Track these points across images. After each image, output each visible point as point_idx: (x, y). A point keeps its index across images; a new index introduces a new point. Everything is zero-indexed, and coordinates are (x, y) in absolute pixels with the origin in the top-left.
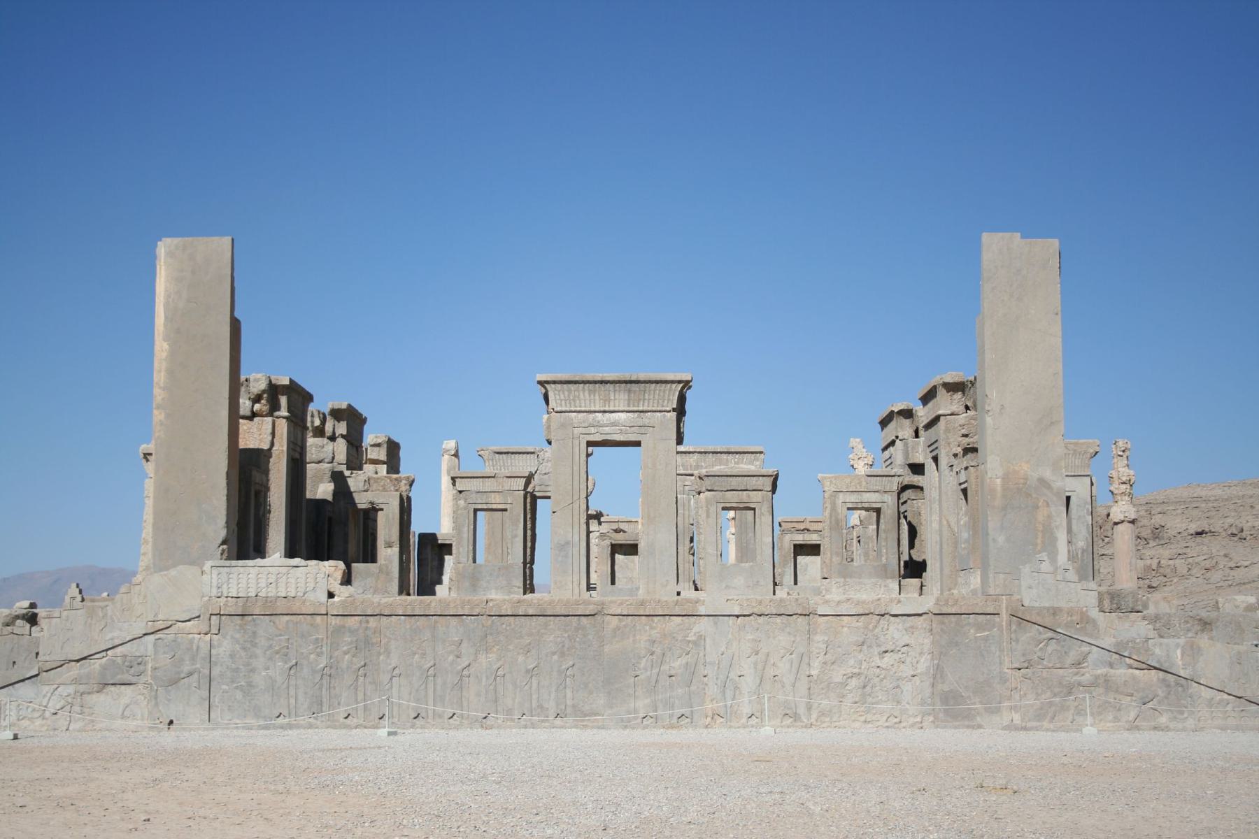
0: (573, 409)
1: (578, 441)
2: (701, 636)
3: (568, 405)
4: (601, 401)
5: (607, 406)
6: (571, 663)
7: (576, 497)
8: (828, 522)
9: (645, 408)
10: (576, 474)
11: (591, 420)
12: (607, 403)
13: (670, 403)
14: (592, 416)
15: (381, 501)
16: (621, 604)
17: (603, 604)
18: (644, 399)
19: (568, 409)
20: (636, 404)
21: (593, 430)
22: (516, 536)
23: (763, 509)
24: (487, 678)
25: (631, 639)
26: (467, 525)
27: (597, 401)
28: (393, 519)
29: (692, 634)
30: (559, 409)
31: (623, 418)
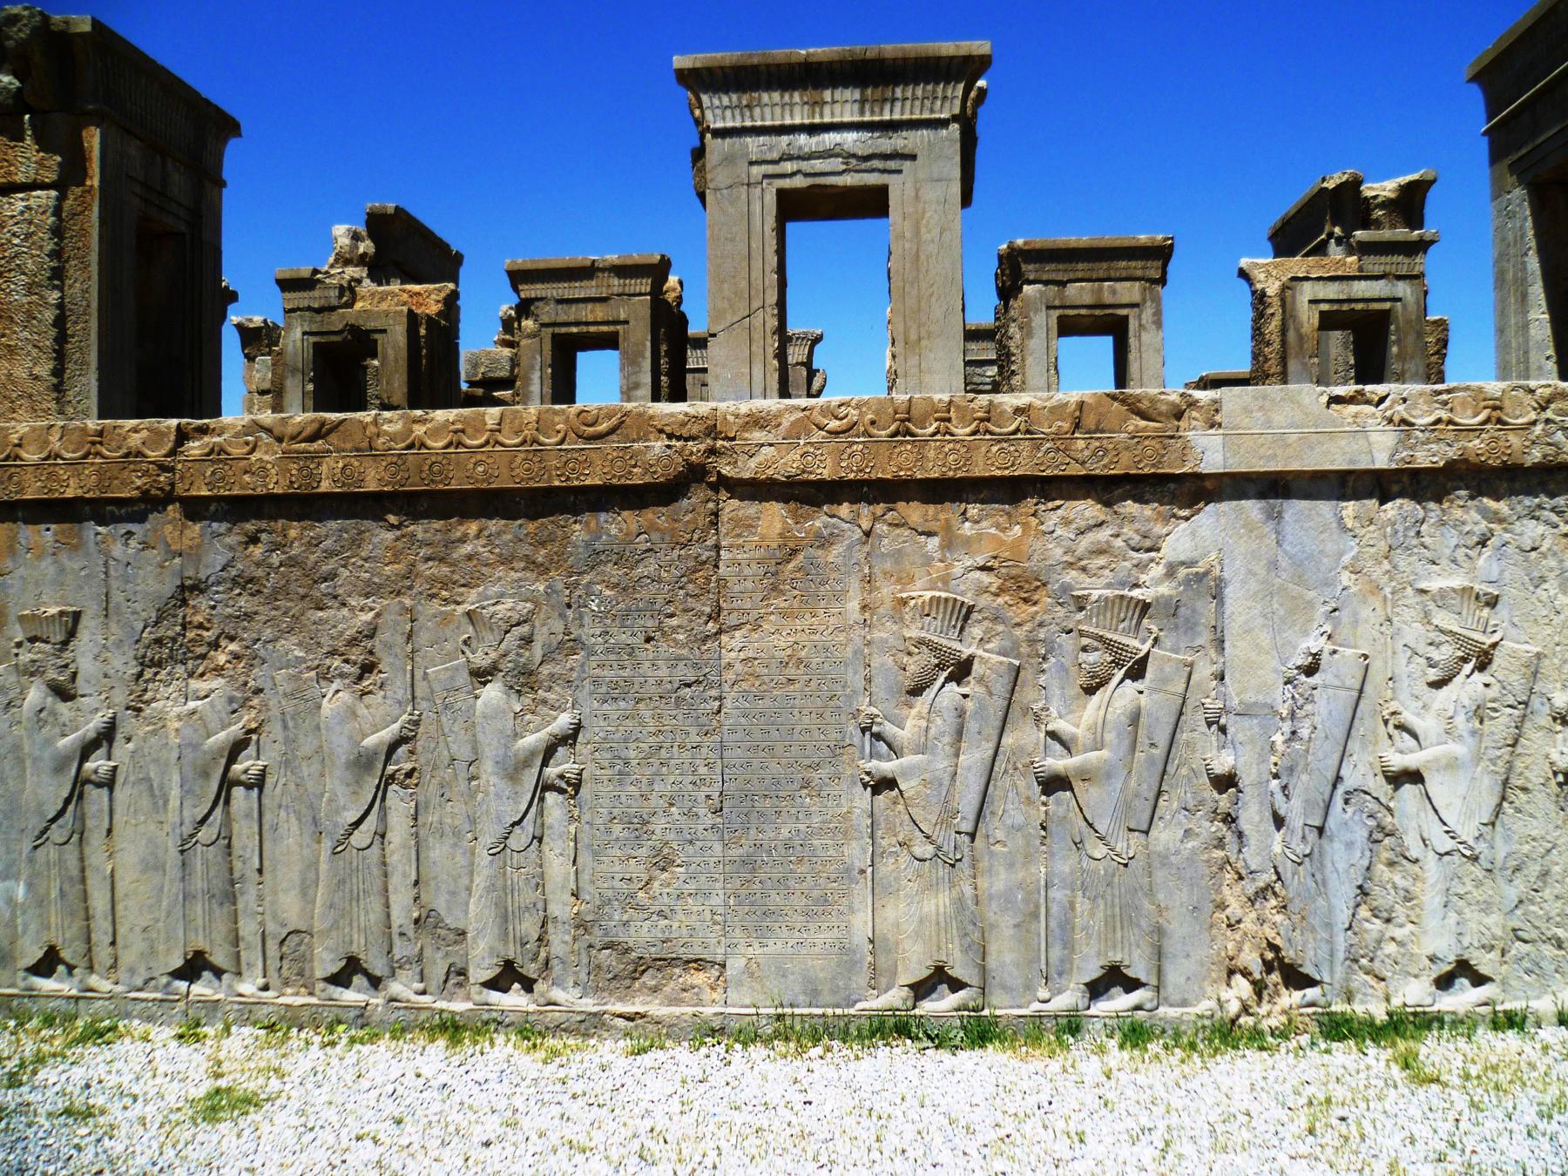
0: (748, 123)
1: (758, 191)
2: (1200, 577)
3: (738, 117)
4: (806, 107)
5: (817, 116)
6: (563, 721)
7: (756, 304)
8: (1277, 345)
9: (896, 116)
10: (757, 255)
11: (784, 145)
12: (817, 110)
13: (947, 105)
14: (785, 139)
15: (371, 325)
16: (798, 430)
17: (712, 431)
18: (894, 100)
19: (738, 124)
20: (877, 109)
21: (789, 167)
22: (637, 386)
23: (1144, 316)
24: (186, 792)
25: (853, 605)
26: (538, 367)
27: (797, 109)
28: (396, 360)
29: (1157, 571)
30: (719, 125)
31: (850, 140)
